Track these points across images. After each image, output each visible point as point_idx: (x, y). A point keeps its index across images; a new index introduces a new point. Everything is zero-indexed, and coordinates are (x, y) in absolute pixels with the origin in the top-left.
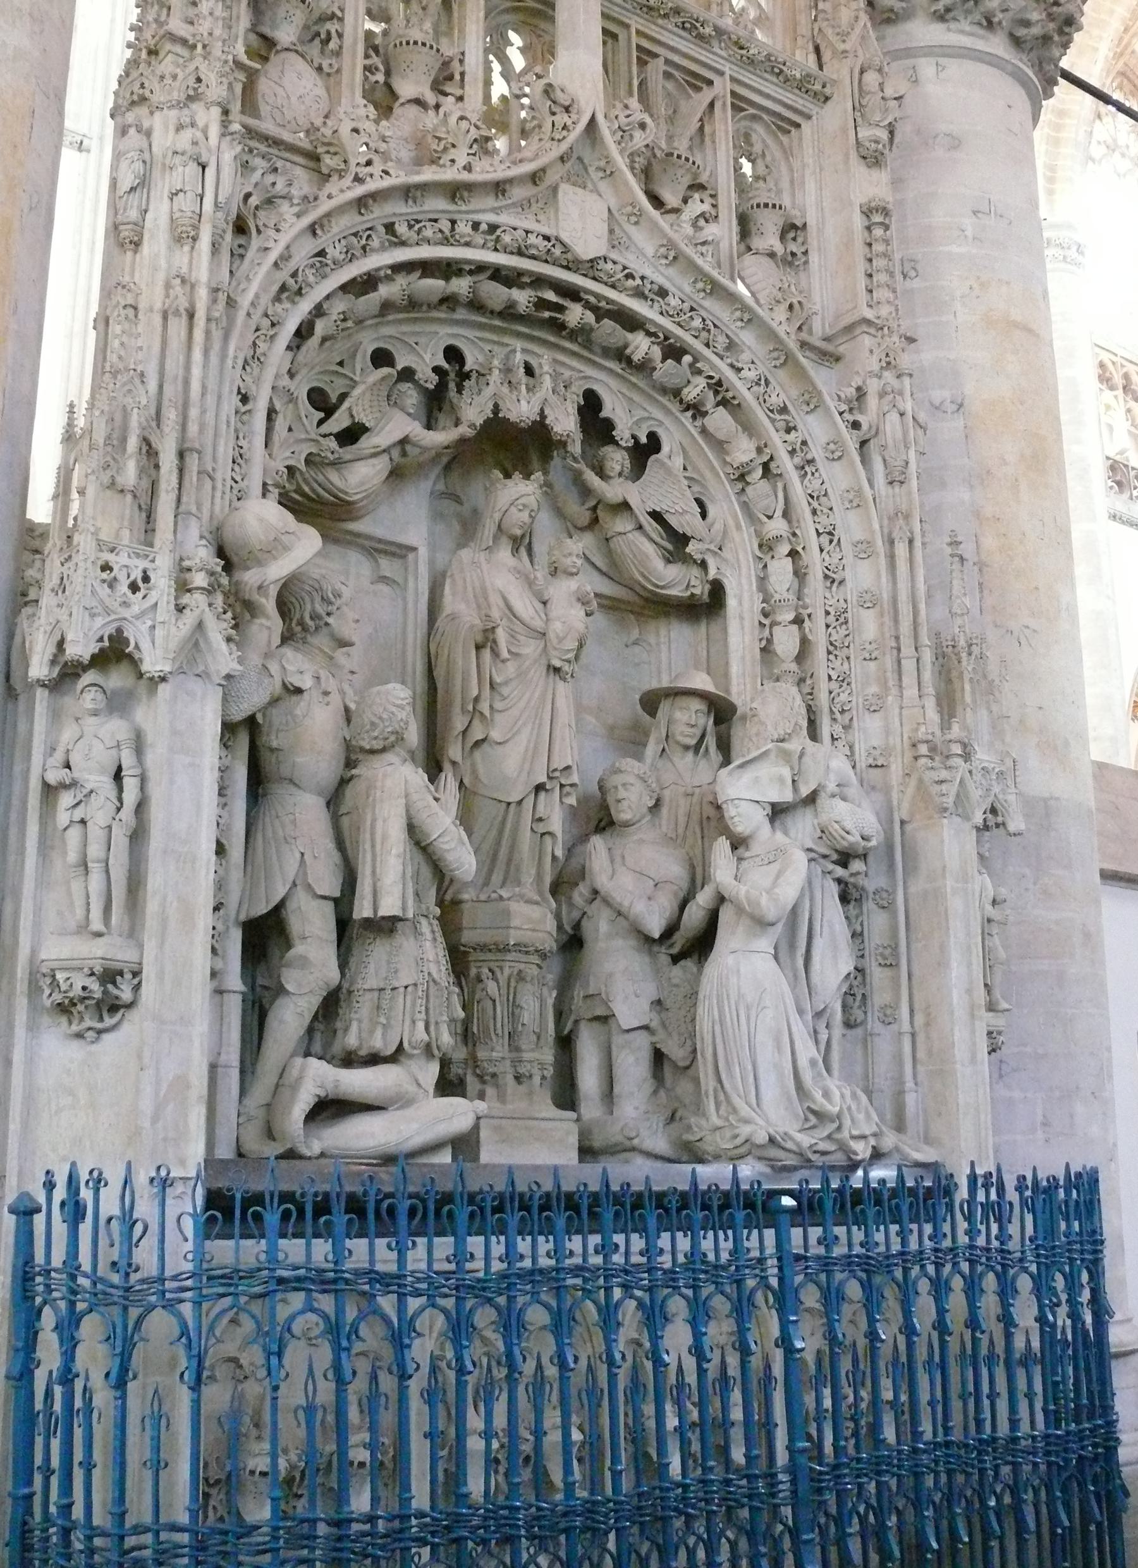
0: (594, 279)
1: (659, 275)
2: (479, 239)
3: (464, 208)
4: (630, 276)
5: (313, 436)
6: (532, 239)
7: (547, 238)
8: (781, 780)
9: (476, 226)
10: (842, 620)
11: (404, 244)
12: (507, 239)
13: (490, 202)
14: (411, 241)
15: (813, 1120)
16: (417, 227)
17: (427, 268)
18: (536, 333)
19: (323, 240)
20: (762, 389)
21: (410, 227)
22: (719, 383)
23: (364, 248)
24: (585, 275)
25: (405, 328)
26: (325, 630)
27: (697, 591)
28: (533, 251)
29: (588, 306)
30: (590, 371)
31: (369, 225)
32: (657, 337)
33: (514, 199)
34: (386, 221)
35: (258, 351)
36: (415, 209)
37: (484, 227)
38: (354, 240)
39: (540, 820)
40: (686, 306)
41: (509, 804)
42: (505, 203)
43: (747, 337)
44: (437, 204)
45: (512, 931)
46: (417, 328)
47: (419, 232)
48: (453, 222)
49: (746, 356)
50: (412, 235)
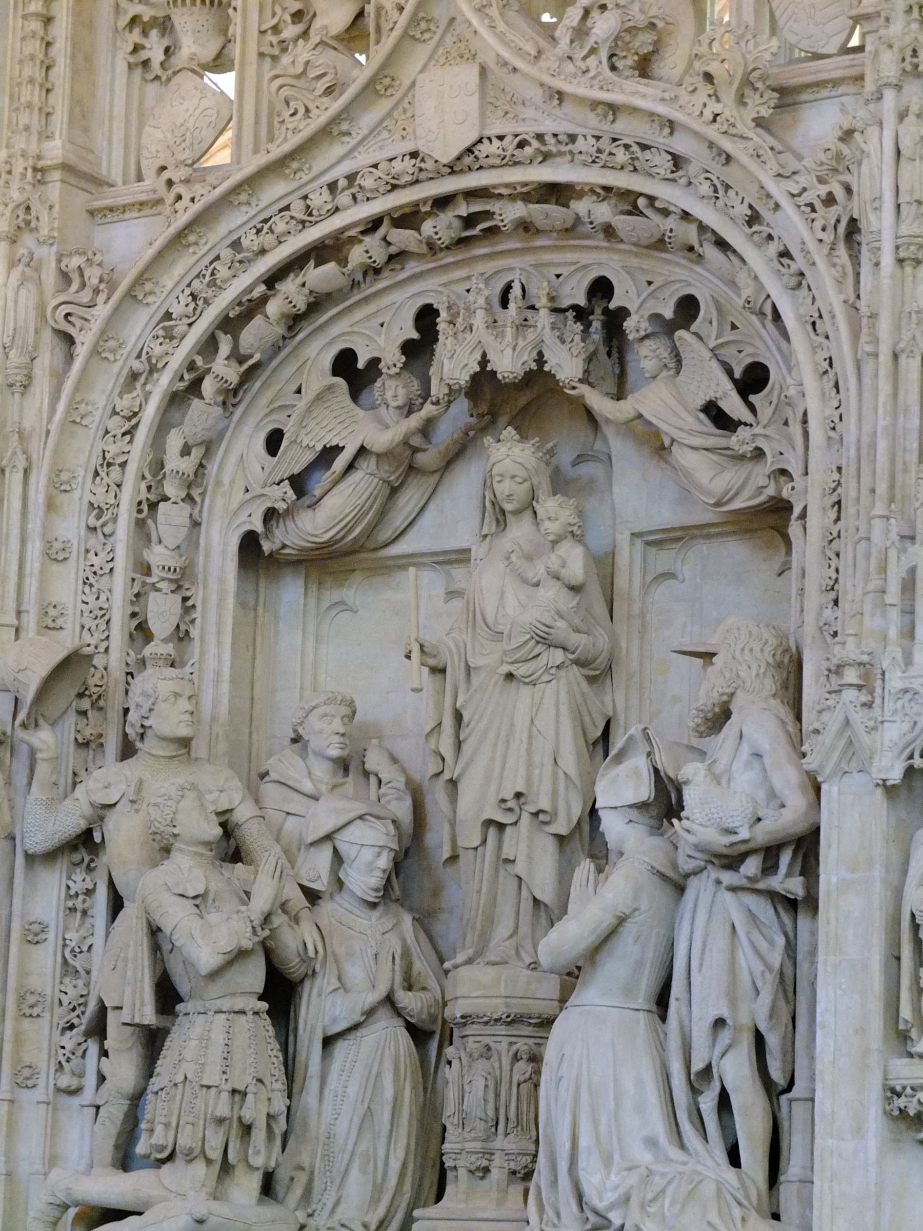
0: (492, 167)
1: (553, 123)
2: (344, 199)
3: (305, 178)
4: (522, 145)
5: (260, 491)
6: (398, 166)
7: (414, 155)
8: (637, 772)
9: (332, 187)
10: (835, 498)
11: (263, 252)
12: (368, 182)
13: (337, 150)
14: (267, 247)
15: (593, 1219)
16: (266, 227)
17: (320, 252)
18: (498, 248)
19: (156, 304)
20: (720, 203)
21: (259, 231)
22: (686, 216)
23: (213, 284)
24: (481, 168)
25: (359, 314)
26: (149, 733)
27: (771, 491)
28: (408, 178)
29: (512, 198)
30: (585, 258)
31: (211, 257)
32: (598, 195)
33: (365, 131)
34: (229, 241)
35: (108, 456)
36: (252, 213)
37: (342, 183)
38: (196, 284)
39: (507, 861)
40: (605, 144)
41: (476, 849)
42: (353, 142)
43: (681, 144)
44: (275, 190)
45: (460, 1001)
46: (371, 308)
47: (271, 230)
48: (305, 197)
49: (693, 169)
50: (267, 239)
